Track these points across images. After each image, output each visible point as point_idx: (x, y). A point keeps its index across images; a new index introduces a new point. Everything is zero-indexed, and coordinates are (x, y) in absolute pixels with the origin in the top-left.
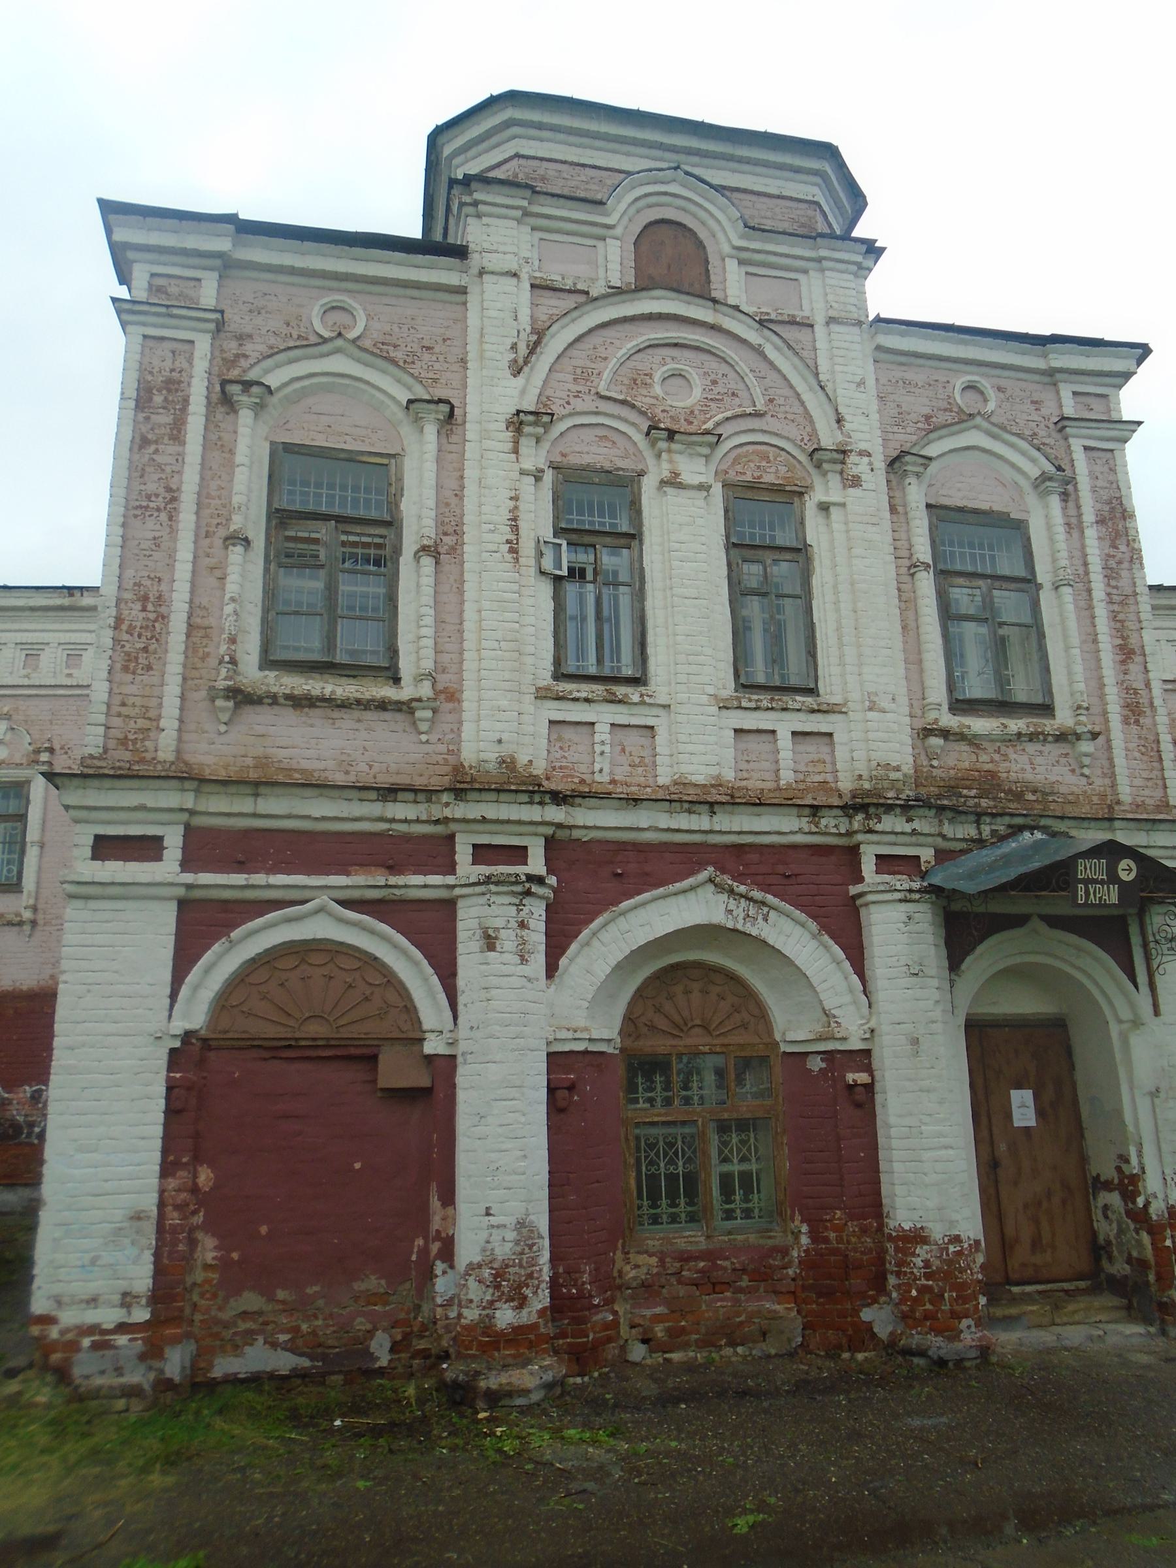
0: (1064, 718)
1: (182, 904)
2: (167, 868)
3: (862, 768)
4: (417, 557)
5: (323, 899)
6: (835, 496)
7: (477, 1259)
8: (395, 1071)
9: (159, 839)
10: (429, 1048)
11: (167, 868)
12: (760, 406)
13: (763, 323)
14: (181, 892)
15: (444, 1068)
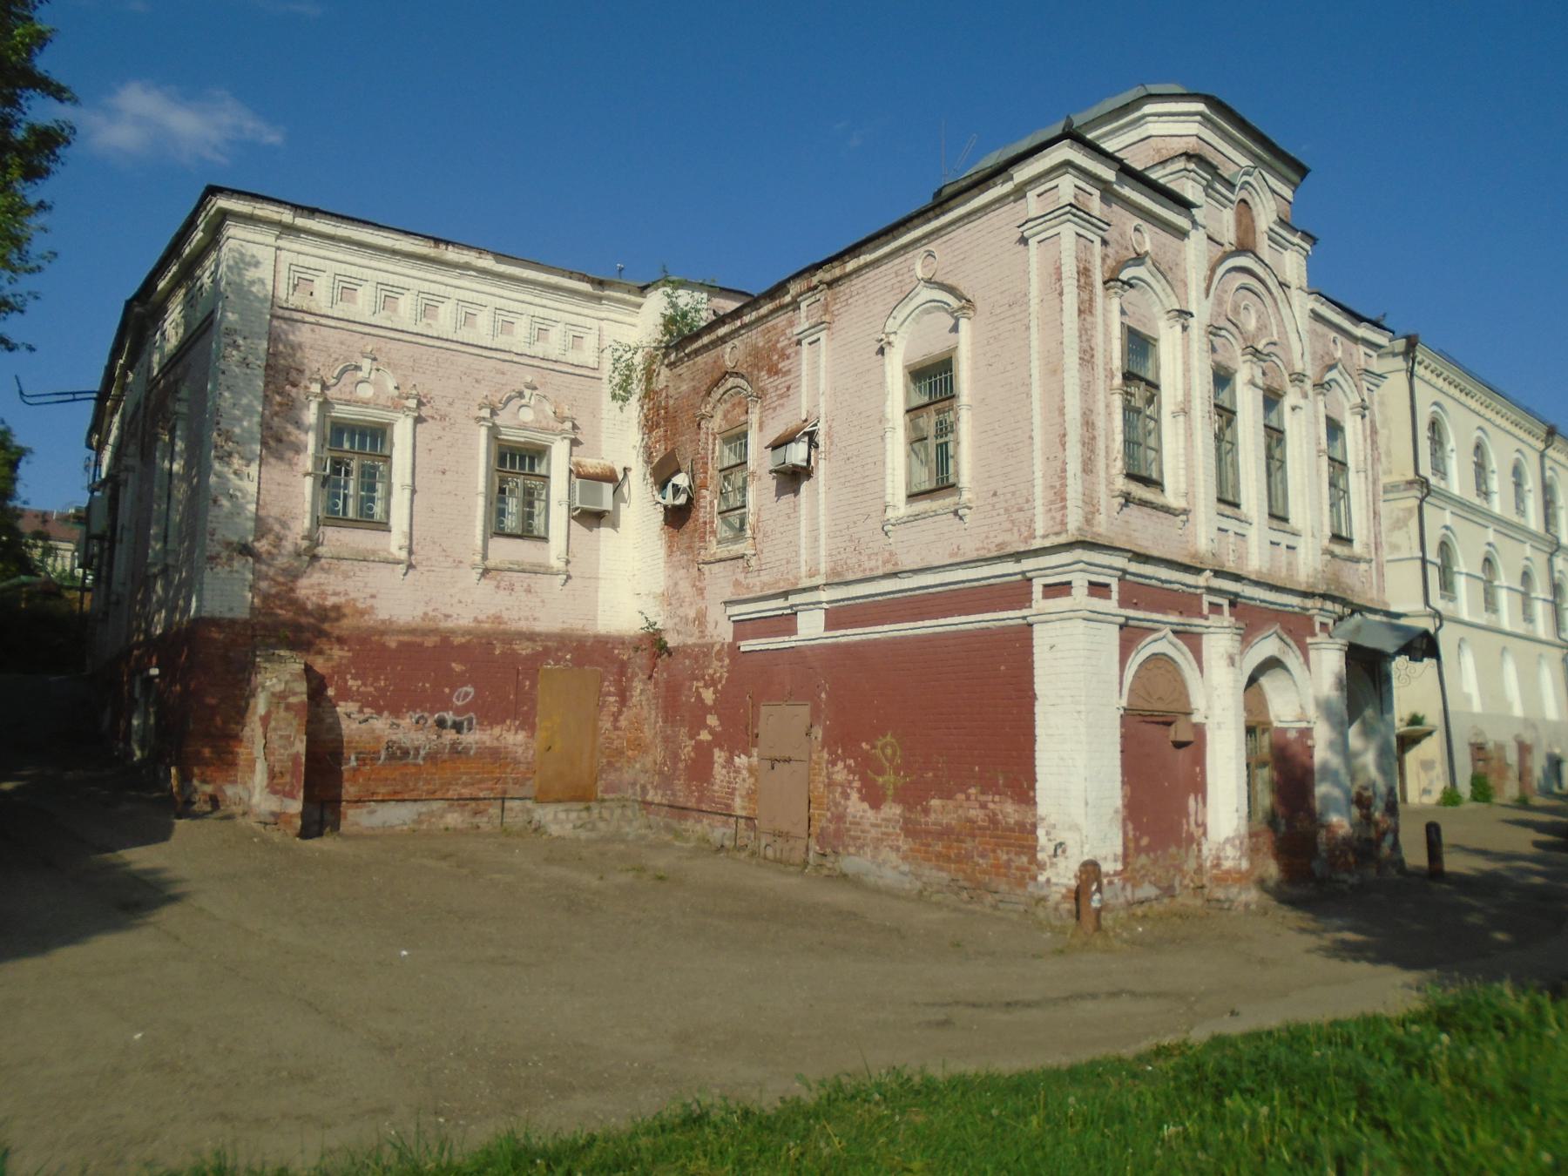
0: (1358, 548)
1: (1122, 627)
2: (1111, 605)
3: (1311, 571)
4: (1175, 415)
5: (1167, 630)
6: (1302, 402)
7: (1231, 834)
8: (1181, 732)
9: (1107, 586)
10: (1196, 718)
11: (1111, 605)
12: (1275, 338)
13: (1281, 284)
14: (1122, 620)
15: (1199, 730)
